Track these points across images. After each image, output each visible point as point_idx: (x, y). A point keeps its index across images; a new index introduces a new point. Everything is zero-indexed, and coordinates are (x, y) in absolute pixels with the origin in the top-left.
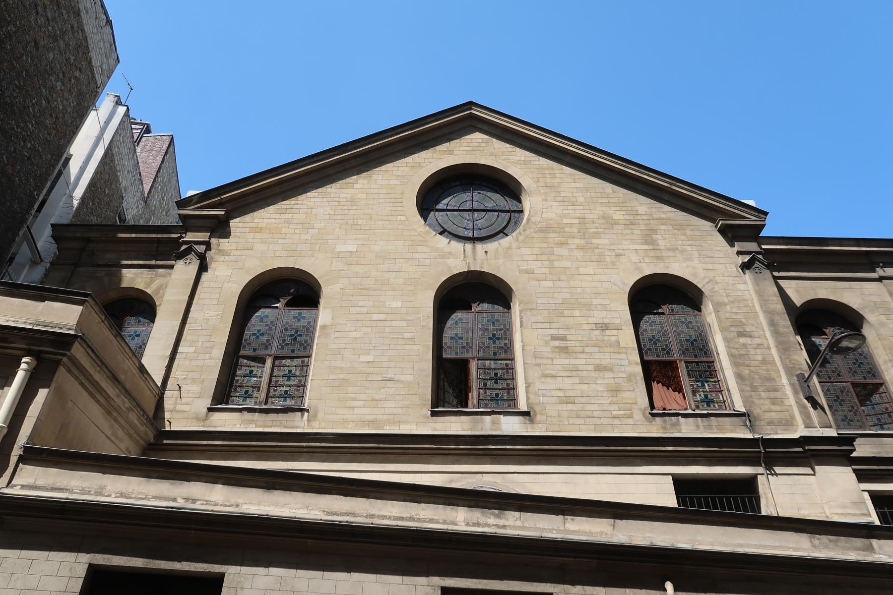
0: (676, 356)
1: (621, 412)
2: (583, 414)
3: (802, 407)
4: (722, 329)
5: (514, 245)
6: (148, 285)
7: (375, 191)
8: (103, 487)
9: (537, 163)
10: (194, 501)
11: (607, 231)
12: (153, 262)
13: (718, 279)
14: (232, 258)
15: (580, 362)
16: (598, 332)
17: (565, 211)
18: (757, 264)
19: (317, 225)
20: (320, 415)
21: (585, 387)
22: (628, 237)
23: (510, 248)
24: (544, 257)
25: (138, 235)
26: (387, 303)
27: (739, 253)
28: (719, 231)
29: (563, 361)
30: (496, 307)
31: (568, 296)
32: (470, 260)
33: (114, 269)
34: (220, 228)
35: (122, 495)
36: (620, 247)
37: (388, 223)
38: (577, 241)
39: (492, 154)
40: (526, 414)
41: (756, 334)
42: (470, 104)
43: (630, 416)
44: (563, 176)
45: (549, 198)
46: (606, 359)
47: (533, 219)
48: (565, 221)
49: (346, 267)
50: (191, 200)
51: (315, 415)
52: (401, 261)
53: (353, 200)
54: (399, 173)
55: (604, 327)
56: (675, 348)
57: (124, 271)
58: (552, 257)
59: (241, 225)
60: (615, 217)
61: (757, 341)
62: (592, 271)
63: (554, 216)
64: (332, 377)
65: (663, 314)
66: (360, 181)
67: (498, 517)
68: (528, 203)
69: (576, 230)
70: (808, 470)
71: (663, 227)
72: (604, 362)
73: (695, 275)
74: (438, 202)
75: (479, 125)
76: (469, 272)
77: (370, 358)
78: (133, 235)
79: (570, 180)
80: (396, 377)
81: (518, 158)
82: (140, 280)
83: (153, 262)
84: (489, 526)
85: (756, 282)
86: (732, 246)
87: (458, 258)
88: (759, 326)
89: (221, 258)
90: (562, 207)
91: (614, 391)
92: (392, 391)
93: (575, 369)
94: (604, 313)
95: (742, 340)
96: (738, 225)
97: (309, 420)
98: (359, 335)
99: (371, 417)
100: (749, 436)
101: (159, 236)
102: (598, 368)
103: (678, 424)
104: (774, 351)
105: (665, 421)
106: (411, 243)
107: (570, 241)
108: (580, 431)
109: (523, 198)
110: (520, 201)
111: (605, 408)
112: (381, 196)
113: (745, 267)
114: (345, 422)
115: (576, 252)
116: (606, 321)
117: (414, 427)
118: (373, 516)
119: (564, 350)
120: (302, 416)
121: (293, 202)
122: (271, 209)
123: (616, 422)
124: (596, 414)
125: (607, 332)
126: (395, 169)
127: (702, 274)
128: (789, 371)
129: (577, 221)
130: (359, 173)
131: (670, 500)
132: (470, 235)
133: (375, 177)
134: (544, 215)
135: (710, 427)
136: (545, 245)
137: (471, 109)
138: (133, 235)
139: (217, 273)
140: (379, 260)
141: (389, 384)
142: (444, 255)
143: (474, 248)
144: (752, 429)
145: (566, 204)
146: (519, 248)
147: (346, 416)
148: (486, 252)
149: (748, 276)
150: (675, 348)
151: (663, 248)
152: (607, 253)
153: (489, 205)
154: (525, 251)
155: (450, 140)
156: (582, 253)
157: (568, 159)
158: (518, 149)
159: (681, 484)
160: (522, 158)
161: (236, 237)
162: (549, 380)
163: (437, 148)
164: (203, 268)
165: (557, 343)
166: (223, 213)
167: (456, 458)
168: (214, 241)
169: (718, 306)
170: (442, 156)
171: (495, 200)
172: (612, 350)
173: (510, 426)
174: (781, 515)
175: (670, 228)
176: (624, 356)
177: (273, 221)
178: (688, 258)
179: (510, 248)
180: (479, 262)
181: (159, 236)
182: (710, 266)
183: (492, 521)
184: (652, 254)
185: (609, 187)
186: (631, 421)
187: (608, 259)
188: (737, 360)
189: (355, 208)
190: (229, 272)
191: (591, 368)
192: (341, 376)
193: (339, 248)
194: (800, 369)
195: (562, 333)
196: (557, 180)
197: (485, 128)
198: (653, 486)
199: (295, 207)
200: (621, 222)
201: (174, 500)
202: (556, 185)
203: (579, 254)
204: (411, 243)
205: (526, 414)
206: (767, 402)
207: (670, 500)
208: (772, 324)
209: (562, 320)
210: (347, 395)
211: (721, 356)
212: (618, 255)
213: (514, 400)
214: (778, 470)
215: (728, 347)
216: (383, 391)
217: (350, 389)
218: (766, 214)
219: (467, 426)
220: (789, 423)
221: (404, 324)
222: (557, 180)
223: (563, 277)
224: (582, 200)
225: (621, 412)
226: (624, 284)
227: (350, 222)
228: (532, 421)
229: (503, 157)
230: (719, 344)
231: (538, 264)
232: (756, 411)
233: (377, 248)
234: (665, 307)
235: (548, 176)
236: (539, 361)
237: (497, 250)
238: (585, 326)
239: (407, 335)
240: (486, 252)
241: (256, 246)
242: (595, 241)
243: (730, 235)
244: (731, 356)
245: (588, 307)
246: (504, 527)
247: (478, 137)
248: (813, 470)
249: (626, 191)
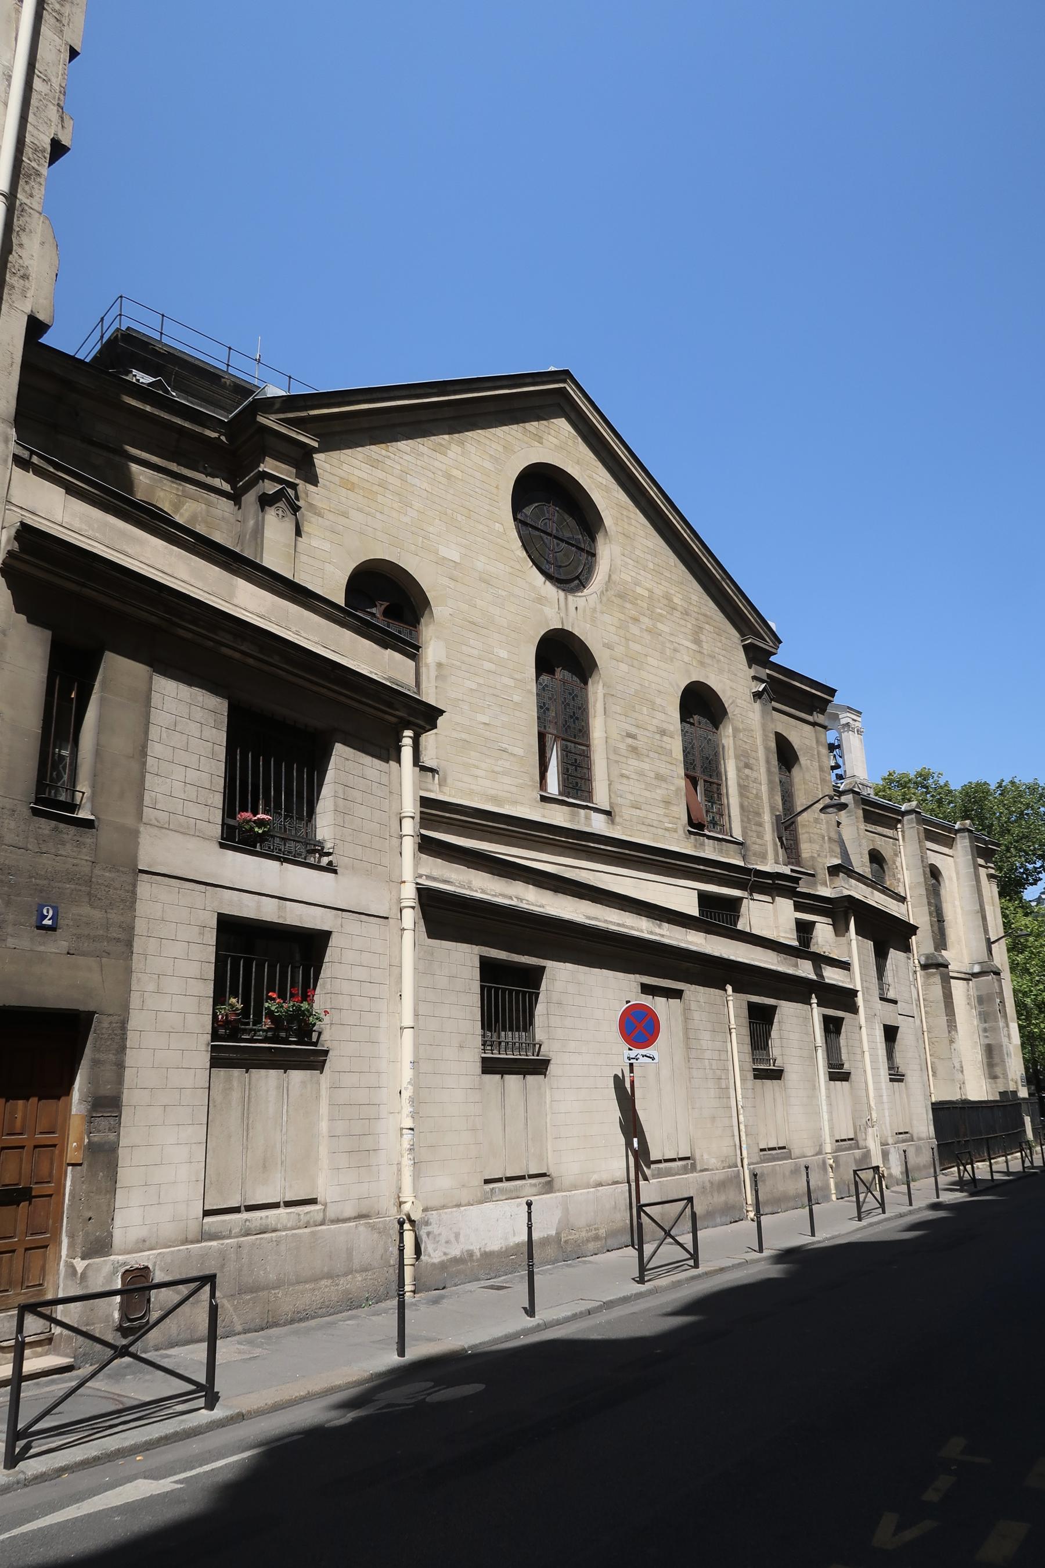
0: (698, 774)
1: (670, 826)
2: (647, 821)
3: (775, 844)
4: (737, 757)
5: (599, 607)
6: (177, 507)
8: (470, 882)
10: (521, 900)
11: (668, 616)
12: (173, 467)
13: (739, 701)
14: (327, 523)
15: (646, 766)
16: (658, 736)
17: (639, 577)
18: (765, 696)
19: (417, 505)
20: (449, 781)
21: (647, 794)
22: (683, 630)
23: (594, 610)
25: (157, 412)
26: (496, 650)
27: (755, 678)
28: (743, 646)
29: (633, 762)
30: (575, 678)
31: (638, 687)
32: (563, 614)
33: (117, 458)
34: (304, 463)
35: (483, 892)
36: (677, 640)
37: (486, 530)
39: (578, 463)
40: (608, 813)
41: (755, 768)
42: (565, 375)
43: (675, 831)
44: (638, 525)
46: (663, 768)
47: (614, 577)
48: (639, 590)
49: (452, 584)
50: (273, 404)
51: (445, 779)
52: (504, 593)
53: (449, 476)
55: (663, 733)
56: (698, 763)
57: (134, 467)
59: (327, 466)
60: (676, 600)
61: (754, 775)
62: (655, 663)
64: (455, 735)
65: (692, 724)
66: (455, 448)
67: (660, 926)
68: (608, 554)
70: (769, 899)
71: (707, 627)
72: (662, 771)
73: (724, 692)
74: (521, 511)
75: (567, 409)
76: (562, 630)
77: (485, 719)
78: (148, 408)
79: (642, 533)
80: (510, 749)
81: (600, 480)
82: (162, 494)
83: (173, 467)
84: (656, 934)
85: (764, 713)
86: (750, 667)
87: (552, 608)
88: (757, 760)
89: (314, 519)
90: (636, 570)
91: (667, 803)
92: (507, 764)
93: (641, 773)
94: (663, 717)
95: (747, 771)
96: (759, 646)
97: (440, 785)
98: (474, 686)
99: (493, 792)
100: (742, 864)
101: (187, 425)
102: (659, 777)
103: (703, 844)
104: (764, 788)
105: (696, 840)
106: (511, 570)
108: (644, 838)
109: (600, 538)
110: (593, 539)
111: (660, 819)
113: (757, 695)
114: (471, 793)
115: (646, 635)
116: (665, 726)
117: (528, 810)
118: (606, 921)
119: (634, 750)
120: (434, 777)
121: (384, 452)
122: (361, 452)
123: (667, 834)
124: (655, 823)
125: (665, 738)
126: (488, 442)
127: (729, 693)
128: (773, 808)
129: (646, 594)
130: (450, 432)
131: (694, 911)
133: (470, 447)
134: (623, 576)
135: (721, 851)
136: (622, 617)
137: (565, 381)
138: (148, 408)
139: (314, 543)
140: (483, 584)
141: (505, 755)
142: (541, 600)
144: (744, 858)
146: (602, 613)
147: (473, 787)
149: (757, 706)
150: (698, 763)
151: (705, 652)
152: (668, 645)
153: (567, 534)
154: (607, 618)
155: (539, 418)
156: (649, 637)
159: (704, 898)
161: (325, 487)
162: (625, 781)
163: (527, 425)
164: (298, 533)
165: (630, 741)
166: (316, 445)
167: (561, 849)
168: (302, 485)
169: (736, 730)
171: (571, 529)
172: (668, 759)
173: (598, 824)
174: (753, 932)
175: (711, 629)
176: (673, 768)
177: (365, 476)
178: (721, 671)
180: (570, 620)
181: (187, 425)
182: (734, 685)
183: (657, 930)
184: (698, 656)
185: (672, 559)
186: (675, 835)
187: (668, 652)
188: (743, 789)
189: (451, 491)
190: (327, 546)
191: (652, 775)
192: (464, 736)
193: (445, 552)
194: (778, 810)
195: (633, 730)
197: (573, 416)
198: (682, 896)
199: (388, 462)
200: (679, 608)
201: (511, 898)
203: (647, 636)
205: (608, 813)
206: (755, 835)
207: (694, 911)
208: (768, 762)
209: (635, 715)
210: (470, 761)
211: (730, 783)
212: (675, 650)
213: (589, 795)
214: (756, 896)
215: (738, 776)
216: (500, 762)
217: (473, 753)
218: (780, 642)
219: (568, 817)
220: (763, 857)
221: (511, 683)
222: (632, 529)
223: (636, 663)
224: (651, 566)
225: (670, 826)
226: (678, 685)
227: (449, 512)
228: (613, 822)
230: (730, 769)
231: (616, 638)
232: (749, 842)
234: (696, 717)
236: (617, 758)
238: (650, 728)
239: (516, 698)
241: (353, 513)
242: (660, 626)
243: (751, 655)
244: (739, 785)
245: (653, 707)
246: (663, 936)
247: (562, 426)
248: (773, 899)
249: (684, 568)
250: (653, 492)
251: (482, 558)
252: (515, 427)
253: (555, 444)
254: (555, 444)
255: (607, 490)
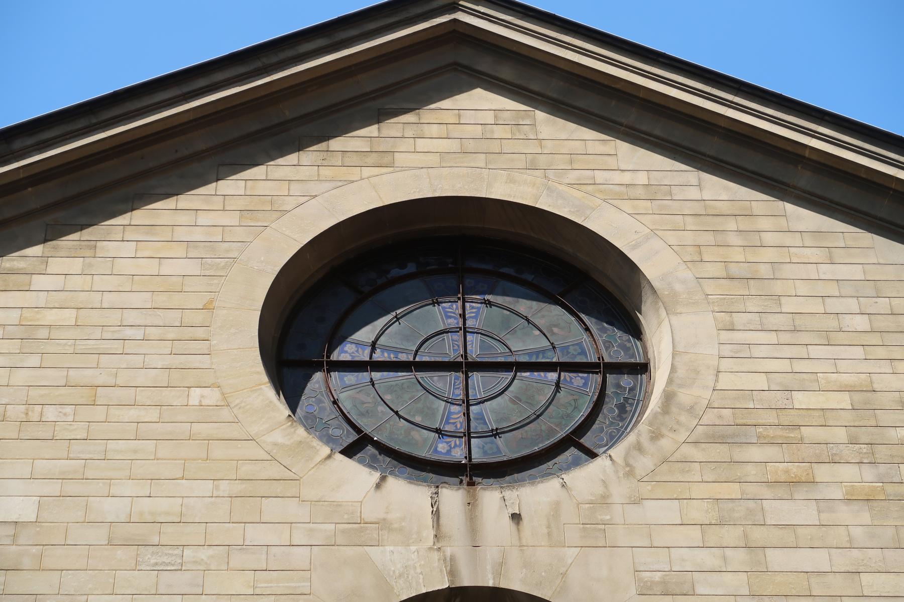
5: (619, 491)
7: (109, 299)
9: (693, 193)
17: (800, 366)
23: (604, 501)
24: (730, 535)
32: (456, 547)
38: (848, 473)
39: (532, 167)
44: (788, 239)
45: (740, 320)
47: (684, 396)
48: (801, 400)
54: (198, 235)
58: (758, 535)
63: (761, 382)
66: (56, 265)
69: (841, 435)
74: (337, 338)
75: (485, 64)
81: (627, 178)
90: (788, 352)
106: (238, 488)
107: (822, 472)
109: (648, 319)
110: (635, 331)
112: (131, 317)
115: (844, 514)
126: (183, 218)
129: (844, 401)
132: (458, 455)
133: (110, 248)
134: (726, 381)
136: (733, 490)
142: (363, 531)
143: (472, 504)
145: (805, 338)
146: (637, 501)
148: (516, 518)
153: (525, 345)
154: (659, 511)
155: (380, 116)
157: (804, 179)
158: (623, 147)
160: (642, 178)
163: (336, 144)
170: (355, 173)
171: (547, 326)
179: (604, 501)
196: (769, 255)
197: (506, 72)
202: (764, 271)
204: (238, 488)
222: (769, 255)
229: (572, 176)
233: (112, 508)
235: (734, 239)
237: (556, 507)
240: (516, 518)
247: (480, 105)
250: (819, 141)
251: (129, 488)
252: (292, 158)
253: (465, 148)
254: (465, 148)
255: (652, 193)
